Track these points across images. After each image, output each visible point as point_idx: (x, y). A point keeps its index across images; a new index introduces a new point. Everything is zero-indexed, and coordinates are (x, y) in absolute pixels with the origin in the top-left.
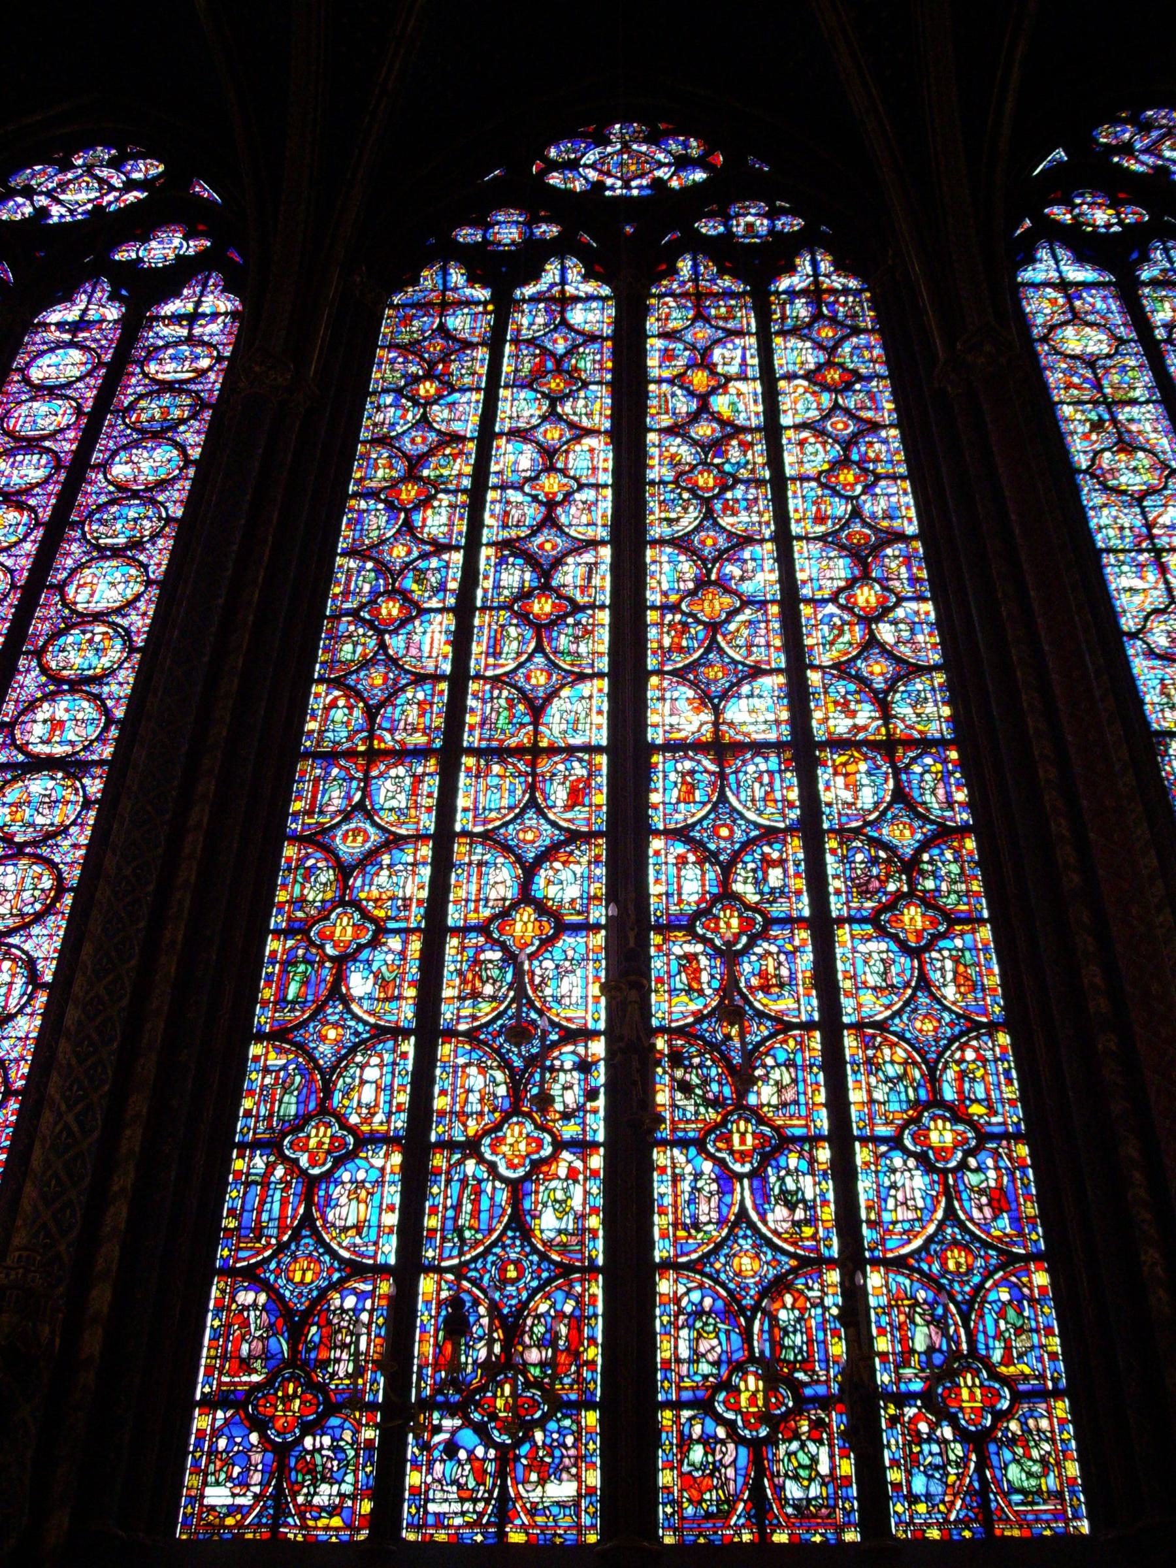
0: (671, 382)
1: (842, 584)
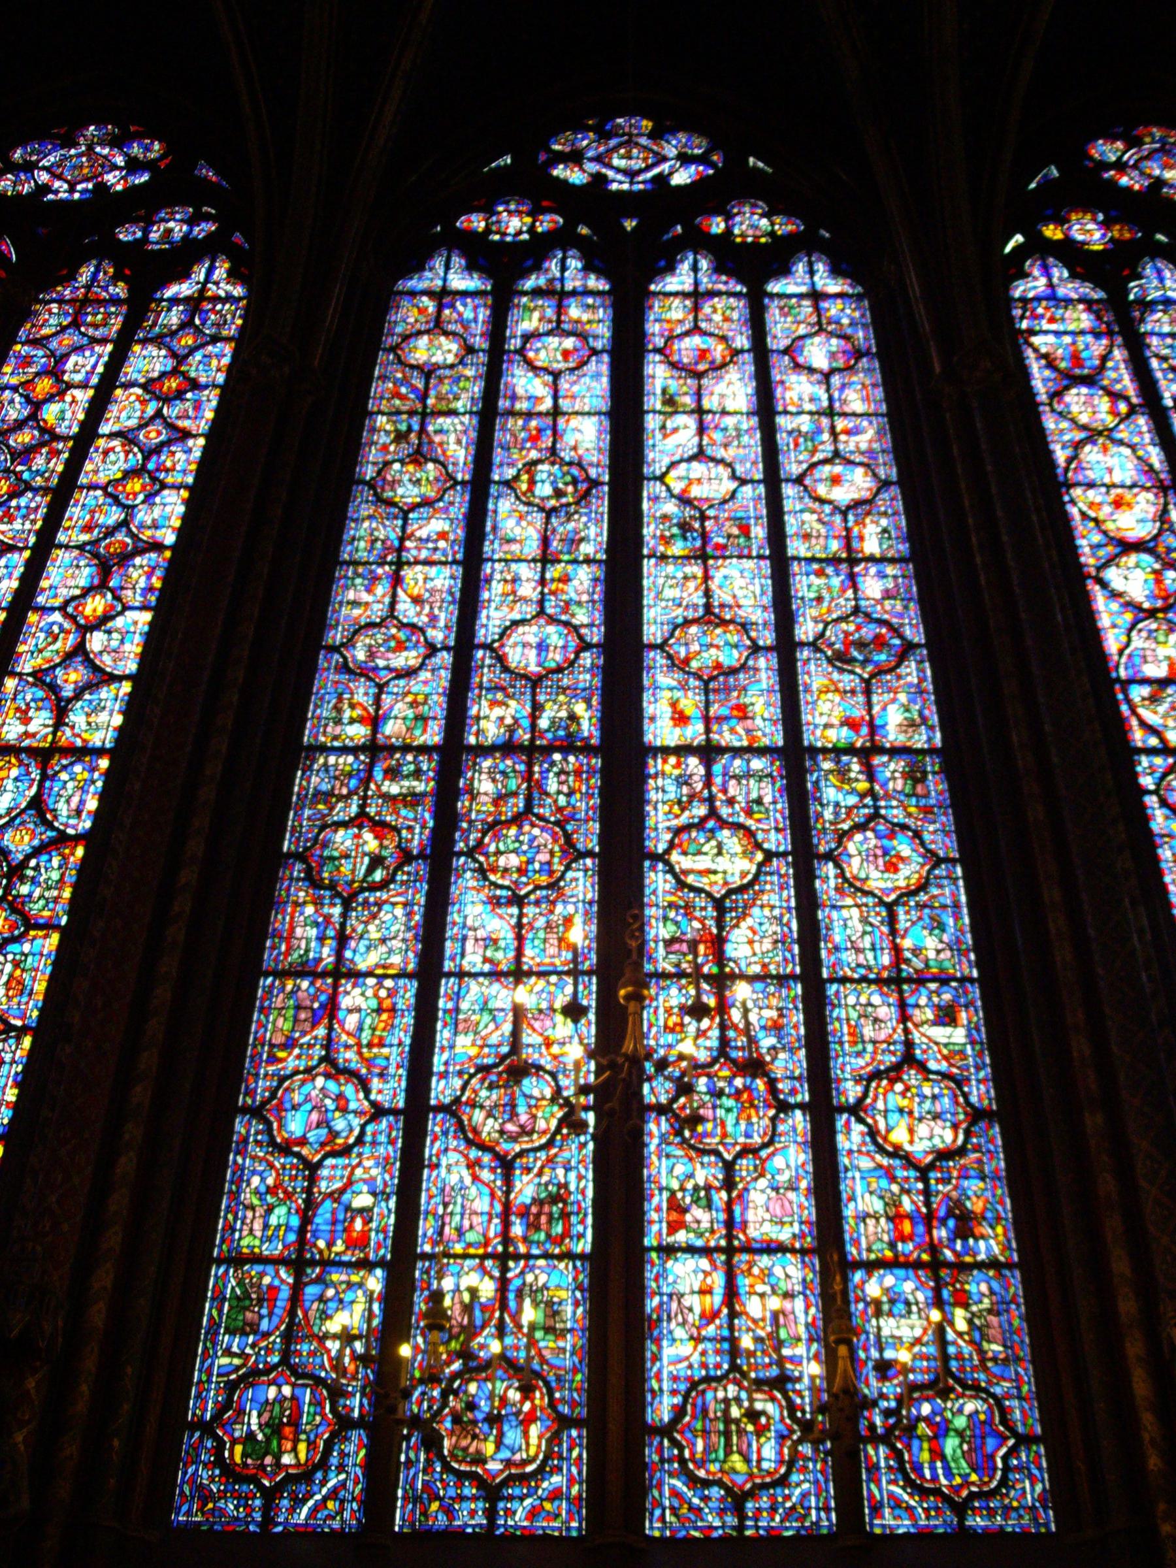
0: (14, 389)
1: (77, 592)
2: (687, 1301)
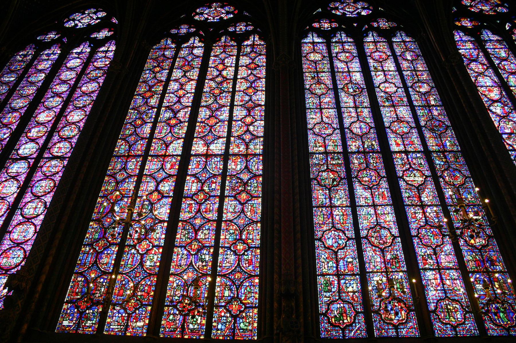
0: (214, 68)
2: (432, 281)
